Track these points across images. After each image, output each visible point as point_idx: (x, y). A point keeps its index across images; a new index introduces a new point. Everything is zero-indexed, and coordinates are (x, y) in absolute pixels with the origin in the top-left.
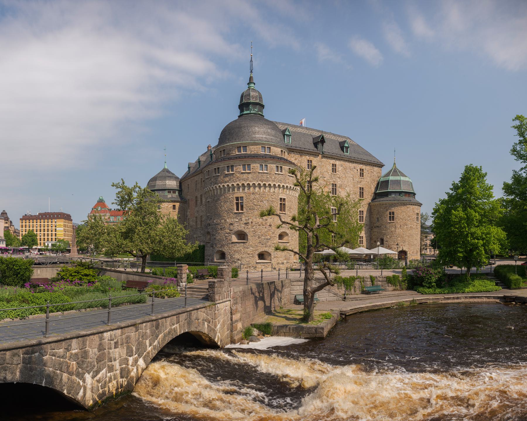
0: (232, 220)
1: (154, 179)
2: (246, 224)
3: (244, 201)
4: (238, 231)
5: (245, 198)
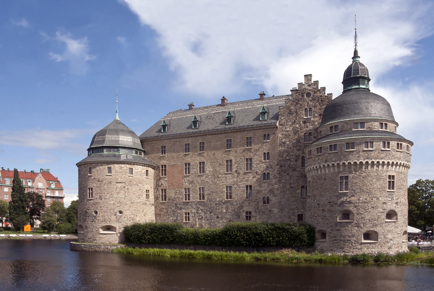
0: (385, 199)
1: (103, 133)
2: (396, 203)
3: (395, 180)
4: (346, 210)
5: (396, 177)
